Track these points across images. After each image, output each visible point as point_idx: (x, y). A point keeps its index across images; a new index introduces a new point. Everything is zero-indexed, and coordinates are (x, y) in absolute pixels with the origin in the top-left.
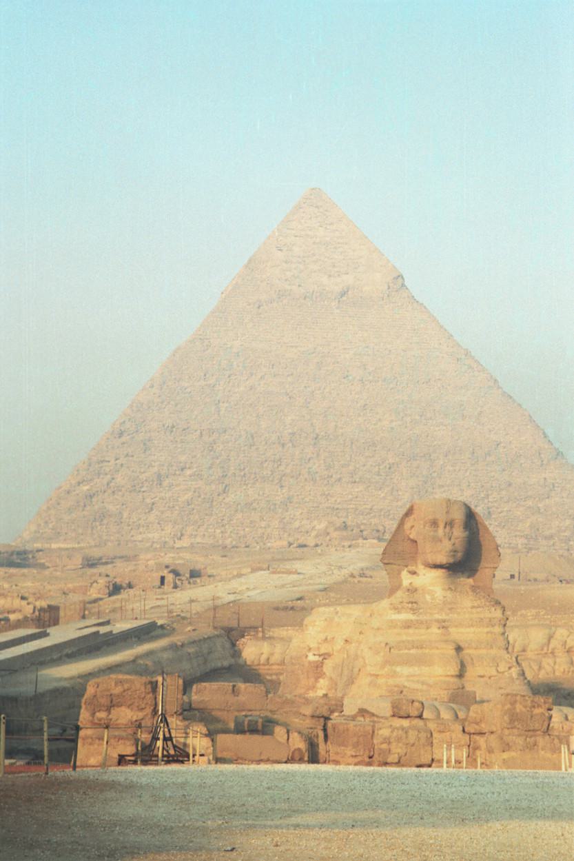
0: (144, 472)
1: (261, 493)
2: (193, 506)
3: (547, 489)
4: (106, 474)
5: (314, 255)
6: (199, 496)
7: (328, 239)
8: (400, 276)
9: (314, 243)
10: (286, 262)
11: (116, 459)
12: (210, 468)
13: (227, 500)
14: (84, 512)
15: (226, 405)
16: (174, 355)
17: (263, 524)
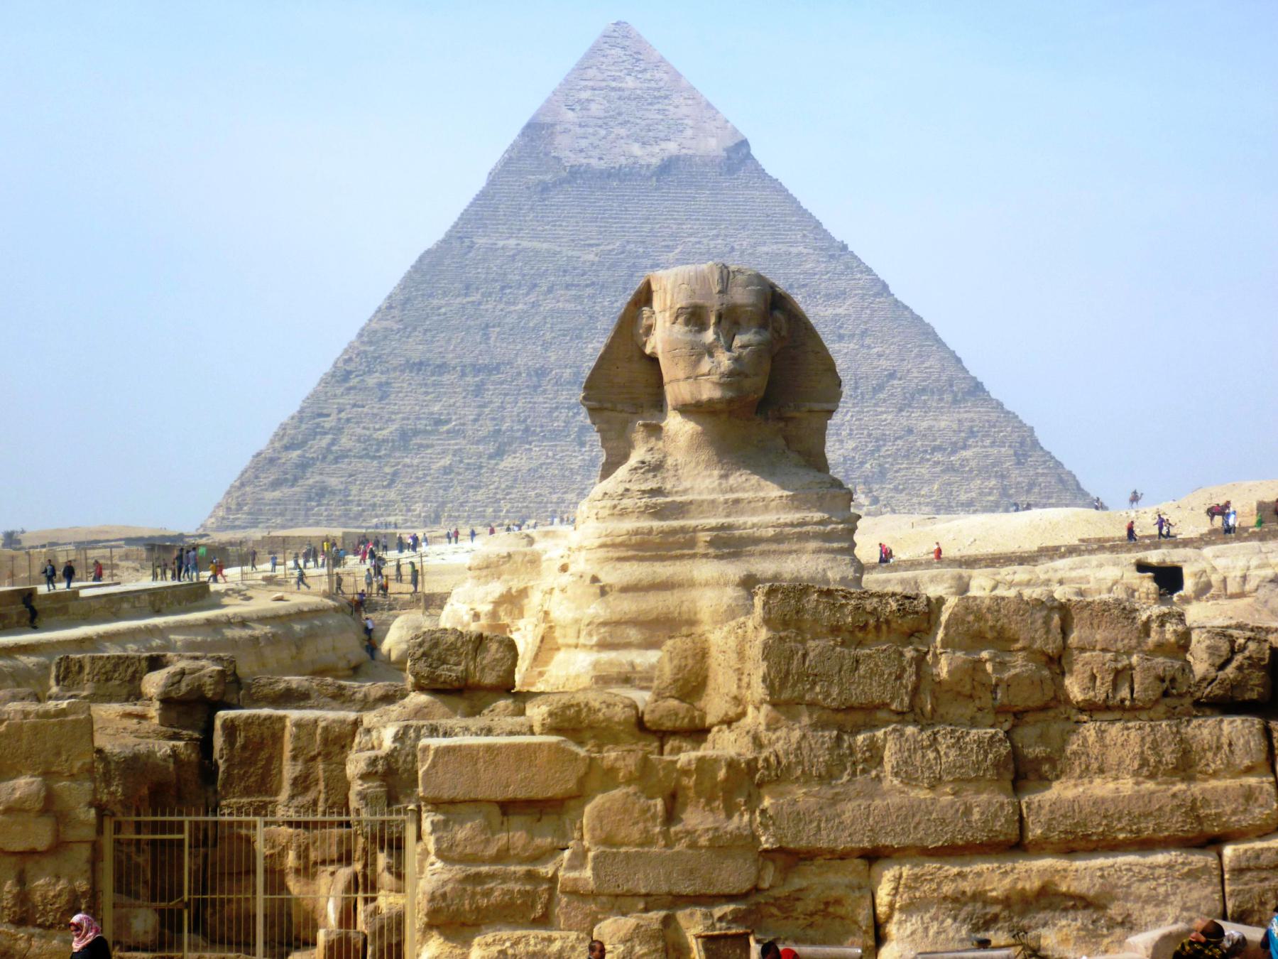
0: (380, 429)
1: (550, 454)
2: (452, 476)
3: (963, 435)
4: (325, 433)
5: (620, 114)
6: (461, 462)
7: (639, 92)
8: (744, 143)
9: (619, 98)
10: (580, 126)
11: (340, 411)
12: (476, 420)
13: (501, 467)
14: (296, 489)
15: (498, 329)
16: (421, 259)
17: (554, 498)
